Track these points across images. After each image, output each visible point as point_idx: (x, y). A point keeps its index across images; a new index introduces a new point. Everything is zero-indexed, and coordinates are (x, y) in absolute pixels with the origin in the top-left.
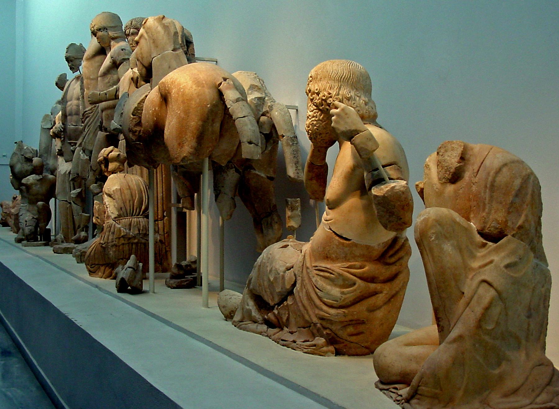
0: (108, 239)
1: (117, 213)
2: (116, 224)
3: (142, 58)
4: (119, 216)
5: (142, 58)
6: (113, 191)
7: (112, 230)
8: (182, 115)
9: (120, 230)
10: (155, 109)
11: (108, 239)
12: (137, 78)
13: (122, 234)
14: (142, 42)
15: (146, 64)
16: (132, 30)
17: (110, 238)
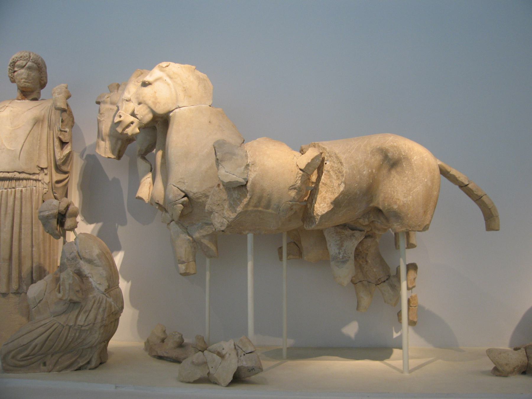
0: (96, 318)
1: (107, 284)
2: (108, 299)
3: (155, 103)
4: (109, 287)
5: (155, 103)
6: (97, 255)
7: (103, 305)
8: (430, 184)
9: (111, 306)
10: (372, 171)
11: (96, 318)
12: (132, 123)
13: (113, 310)
14: (157, 86)
15: (161, 110)
16: (30, 64)
17: (99, 317)
